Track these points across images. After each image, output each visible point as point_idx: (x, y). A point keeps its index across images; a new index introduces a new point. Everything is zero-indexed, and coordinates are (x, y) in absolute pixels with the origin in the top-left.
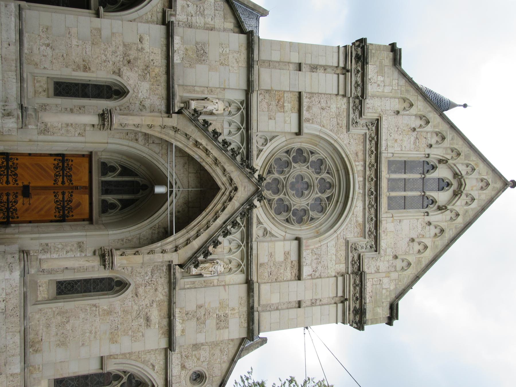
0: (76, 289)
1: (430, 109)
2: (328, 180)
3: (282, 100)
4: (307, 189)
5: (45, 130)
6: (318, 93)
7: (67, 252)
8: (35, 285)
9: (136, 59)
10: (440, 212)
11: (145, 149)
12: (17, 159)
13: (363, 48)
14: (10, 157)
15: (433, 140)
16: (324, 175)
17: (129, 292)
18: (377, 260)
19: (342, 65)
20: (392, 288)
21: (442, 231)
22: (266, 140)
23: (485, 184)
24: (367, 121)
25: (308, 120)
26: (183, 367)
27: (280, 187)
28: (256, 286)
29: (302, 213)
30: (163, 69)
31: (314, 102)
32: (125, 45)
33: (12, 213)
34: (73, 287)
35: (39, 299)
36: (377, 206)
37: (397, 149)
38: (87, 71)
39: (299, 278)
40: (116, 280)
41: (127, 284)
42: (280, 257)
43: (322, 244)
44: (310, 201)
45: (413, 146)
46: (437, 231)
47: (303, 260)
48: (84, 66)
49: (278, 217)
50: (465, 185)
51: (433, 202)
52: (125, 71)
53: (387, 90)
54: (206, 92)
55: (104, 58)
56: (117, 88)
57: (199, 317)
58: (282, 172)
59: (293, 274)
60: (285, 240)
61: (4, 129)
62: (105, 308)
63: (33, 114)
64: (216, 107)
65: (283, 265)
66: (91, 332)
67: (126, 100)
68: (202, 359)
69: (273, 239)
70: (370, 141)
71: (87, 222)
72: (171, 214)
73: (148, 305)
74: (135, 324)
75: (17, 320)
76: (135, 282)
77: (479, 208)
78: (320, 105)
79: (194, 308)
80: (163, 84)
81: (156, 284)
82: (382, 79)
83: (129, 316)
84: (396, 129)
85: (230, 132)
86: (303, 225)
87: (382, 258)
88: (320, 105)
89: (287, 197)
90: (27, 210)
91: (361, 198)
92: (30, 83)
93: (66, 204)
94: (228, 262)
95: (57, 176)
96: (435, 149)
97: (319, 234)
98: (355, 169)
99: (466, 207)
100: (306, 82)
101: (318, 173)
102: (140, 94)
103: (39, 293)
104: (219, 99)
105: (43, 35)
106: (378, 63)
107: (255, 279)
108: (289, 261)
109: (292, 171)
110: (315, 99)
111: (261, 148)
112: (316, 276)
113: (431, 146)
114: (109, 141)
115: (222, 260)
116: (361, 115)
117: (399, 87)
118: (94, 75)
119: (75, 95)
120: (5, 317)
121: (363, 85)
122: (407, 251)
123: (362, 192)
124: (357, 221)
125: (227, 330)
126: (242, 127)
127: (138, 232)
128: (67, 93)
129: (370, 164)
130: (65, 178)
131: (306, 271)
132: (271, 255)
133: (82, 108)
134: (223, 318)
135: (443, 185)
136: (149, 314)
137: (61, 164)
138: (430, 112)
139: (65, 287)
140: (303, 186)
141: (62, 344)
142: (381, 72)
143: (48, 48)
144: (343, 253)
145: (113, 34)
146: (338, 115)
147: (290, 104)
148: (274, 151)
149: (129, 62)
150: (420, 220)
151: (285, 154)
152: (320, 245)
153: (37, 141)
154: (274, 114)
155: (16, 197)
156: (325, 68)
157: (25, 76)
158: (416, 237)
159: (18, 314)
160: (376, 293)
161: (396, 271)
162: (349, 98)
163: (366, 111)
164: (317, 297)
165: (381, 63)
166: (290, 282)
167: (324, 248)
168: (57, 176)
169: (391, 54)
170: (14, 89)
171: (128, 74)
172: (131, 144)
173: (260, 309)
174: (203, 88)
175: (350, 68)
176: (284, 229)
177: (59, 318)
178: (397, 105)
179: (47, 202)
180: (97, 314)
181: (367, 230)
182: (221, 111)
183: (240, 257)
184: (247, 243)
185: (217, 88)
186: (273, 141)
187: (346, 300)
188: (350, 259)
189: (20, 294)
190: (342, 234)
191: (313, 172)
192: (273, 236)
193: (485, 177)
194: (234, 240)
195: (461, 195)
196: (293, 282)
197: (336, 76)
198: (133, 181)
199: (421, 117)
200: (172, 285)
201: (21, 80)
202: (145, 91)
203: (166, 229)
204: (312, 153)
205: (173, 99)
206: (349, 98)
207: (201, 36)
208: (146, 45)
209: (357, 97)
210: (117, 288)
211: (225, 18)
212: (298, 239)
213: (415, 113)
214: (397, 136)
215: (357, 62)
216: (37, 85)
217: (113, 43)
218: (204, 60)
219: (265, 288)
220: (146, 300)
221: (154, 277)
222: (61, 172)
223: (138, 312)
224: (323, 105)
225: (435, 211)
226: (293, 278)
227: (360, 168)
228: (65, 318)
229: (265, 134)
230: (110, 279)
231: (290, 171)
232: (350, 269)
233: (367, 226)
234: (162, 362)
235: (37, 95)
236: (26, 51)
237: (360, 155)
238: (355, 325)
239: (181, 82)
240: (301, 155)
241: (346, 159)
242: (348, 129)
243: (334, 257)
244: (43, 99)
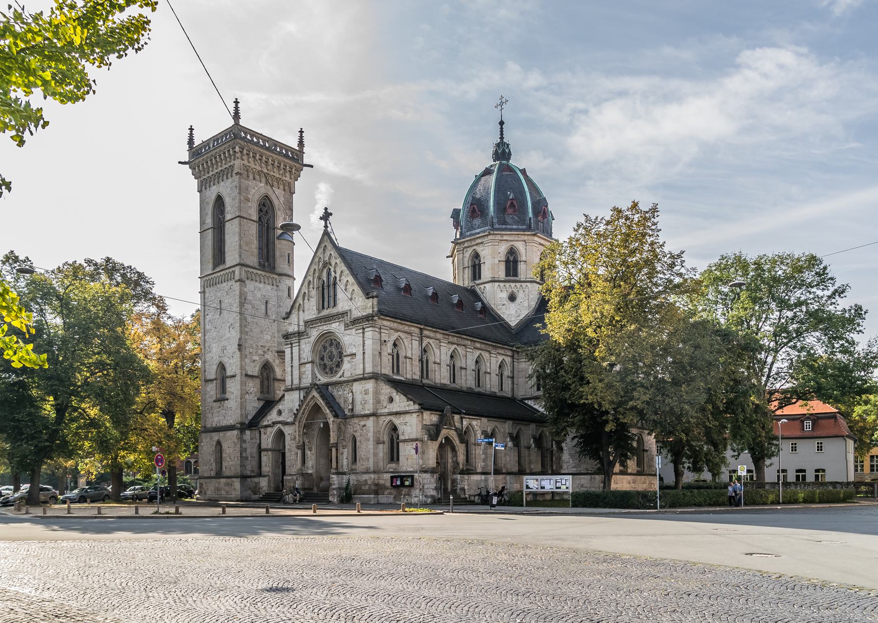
15: (311, 286)
135: (329, 274)
240: (322, 359)
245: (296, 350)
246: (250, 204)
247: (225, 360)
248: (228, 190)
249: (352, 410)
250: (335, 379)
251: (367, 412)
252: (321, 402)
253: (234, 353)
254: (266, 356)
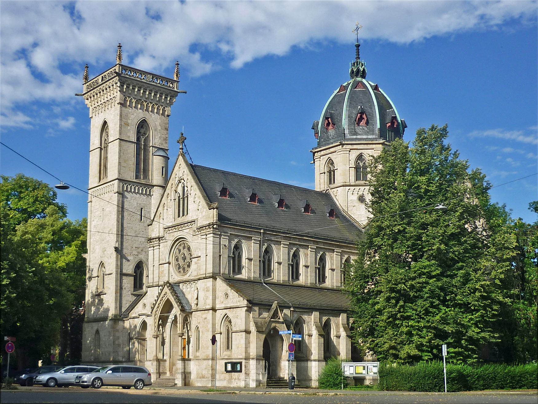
15: (169, 198)
188: (197, 233)
245: (156, 251)
246: (129, 128)
247: (105, 260)
248: (112, 117)
249: (197, 304)
250: (186, 278)
252: (172, 299)
253: (112, 254)
254: (140, 256)
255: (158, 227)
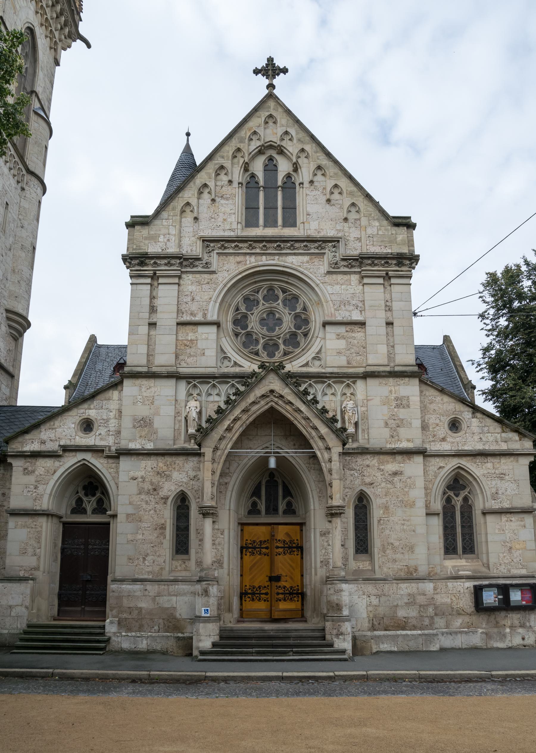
0: (364, 537)
1: (192, 184)
2: (265, 292)
3: (185, 342)
4: (274, 315)
5: (219, 563)
6: (177, 305)
7: (329, 545)
8: (357, 572)
9: (152, 483)
10: (299, 170)
11: (235, 476)
12: (246, 586)
13: (131, 258)
14: (244, 592)
15: (224, 178)
16: (260, 296)
17: (369, 491)
18: (348, 240)
19: (149, 281)
20: (377, 224)
21: (319, 168)
22: (225, 358)
23: (271, 119)
24: (205, 252)
25: (205, 315)
26: (444, 440)
27: (271, 343)
28: (369, 369)
29: (299, 320)
30: (160, 459)
31: (187, 309)
32: (140, 493)
33: (294, 590)
34: (361, 540)
35: (371, 568)
36: (292, 241)
37: (233, 219)
38: (165, 527)
39: (362, 324)
40: (357, 502)
41: (361, 493)
42: (342, 344)
43: (329, 299)
44: (287, 311)
45: (230, 201)
46: (319, 173)
47: (345, 320)
48: (160, 528)
49: (301, 344)
50: (271, 141)
51: (288, 176)
52: (163, 493)
53: (173, 231)
54: (179, 418)
55: (152, 512)
56: (179, 501)
57: (396, 425)
58: (257, 341)
59: (359, 330)
60: (325, 338)
61: (219, 595)
62: (381, 512)
63: (205, 572)
64: (193, 409)
65: (350, 340)
66: (403, 525)
67: (189, 493)
68: (438, 421)
69: (323, 350)
70: (225, 248)
71: (304, 527)
72: (296, 453)
73: (382, 473)
74: (398, 485)
75: (387, 586)
76: (359, 485)
77: (296, 126)
78: (189, 303)
79: (387, 430)
80: (174, 459)
81: (362, 466)
82: (162, 237)
83: (391, 490)
84: (213, 220)
85: (217, 395)
86: (310, 319)
87: (347, 234)
88: (189, 303)
89: (282, 335)
90: (291, 578)
91: (284, 258)
92: (178, 574)
93: (287, 546)
94: (344, 396)
95: (260, 553)
96: (234, 176)
97: (319, 303)
98: (254, 264)
99: (295, 141)
100: (167, 317)
101: (258, 303)
102: (183, 480)
103: (365, 569)
104: (186, 406)
105: (136, 562)
106: (147, 242)
107: (361, 370)
108: (346, 334)
109: (255, 331)
110: (183, 307)
111: (232, 362)
112: (362, 306)
113: (230, 182)
114: (228, 508)
115: (342, 403)
116: (199, 259)
117: (170, 217)
118: (168, 521)
119: (187, 537)
120: (384, 595)
121: (169, 258)
122: (339, 206)
123: (278, 257)
124: (308, 262)
125: (410, 397)
126: (213, 382)
127: (313, 484)
128: (185, 544)
129: (248, 248)
130: (262, 546)
131: (356, 316)
132: (339, 353)
133: (199, 531)
134: (399, 402)
135: (271, 167)
136: (390, 473)
137: (250, 550)
138: (195, 183)
139: (361, 546)
140: (271, 320)
141: (411, 549)
142: (154, 238)
143: (147, 559)
144: (340, 277)
145: (130, 503)
146: (199, 283)
147: (189, 334)
148: (236, 349)
149: (155, 490)
150: (308, 192)
151: (239, 338)
152: (330, 302)
153: (229, 569)
154: (199, 350)
155: (280, 587)
156: (152, 298)
157: (172, 578)
158: (325, 196)
159: (382, 585)
160: (382, 241)
161: (359, 219)
162: (182, 272)
163: (194, 253)
164: (383, 305)
165: (146, 238)
166: (367, 334)
167: (334, 298)
168: (260, 553)
169: (137, 228)
170: (184, 587)
171: (166, 491)
172: (230, 487)
173: (392, 364)
174: (176, 421)
175: (152, 272)
176: (314, 339)
177: (388, 552)
178: (188, 219)
179: (284, 563)
180: (387, 519)
181: (317, 251)
182: (197, 404)
183: (341, 384)
184: (326, 377)
185: (175, 407)
186: (226, 351)
187: (387, 274)
189: (364, 584)
190: (320, 278)
191: (257, 309)
192: (320, 350)
193: (263, 119)
194: (323, 391)
195: (282, 146)
196: (367, 331)
197: (160, 286)
198: (266, 486)
199: (200, 193)
200: (364, 452)
201: (175, 581)
202: (181, 475)
203: (310, 457)
204: (237, 309)
205: (187, 450)
206: (182, 272)
207: (127, 423)
208: (139, 474)
209: (181, 264)
210: (365, 502)
211: (109, 399)
212: (325, 324)
213: (196, 200)
214: (220, 219)
215: (146, 265)
216: (179, 568)
217: (139, 503)
218: (150, 420)
219: (372, 359)
220: (377, 475)
221: (355, 468)
222: (257, 550)
223: (388, 482)
224: (189, 299)
225: (298, 175)
226: (363, 330)
227: (253, 259)
228: (388, 547)
229: (219, 359)
230: (356, 507)
231: (256, 333)
232: (356, 270)
233: (312, 251)
234: (437, 460)
235: (188, 569)
236: (151, 577)
237: (239, 259)
238: (413, 265)
239: (171, 442)
240: (240, 321)
241: (244, 274)
242: (213, 272)
243: (343, 287)
244: (192, 564)
251: (404, 445)
255: (173, 231)
